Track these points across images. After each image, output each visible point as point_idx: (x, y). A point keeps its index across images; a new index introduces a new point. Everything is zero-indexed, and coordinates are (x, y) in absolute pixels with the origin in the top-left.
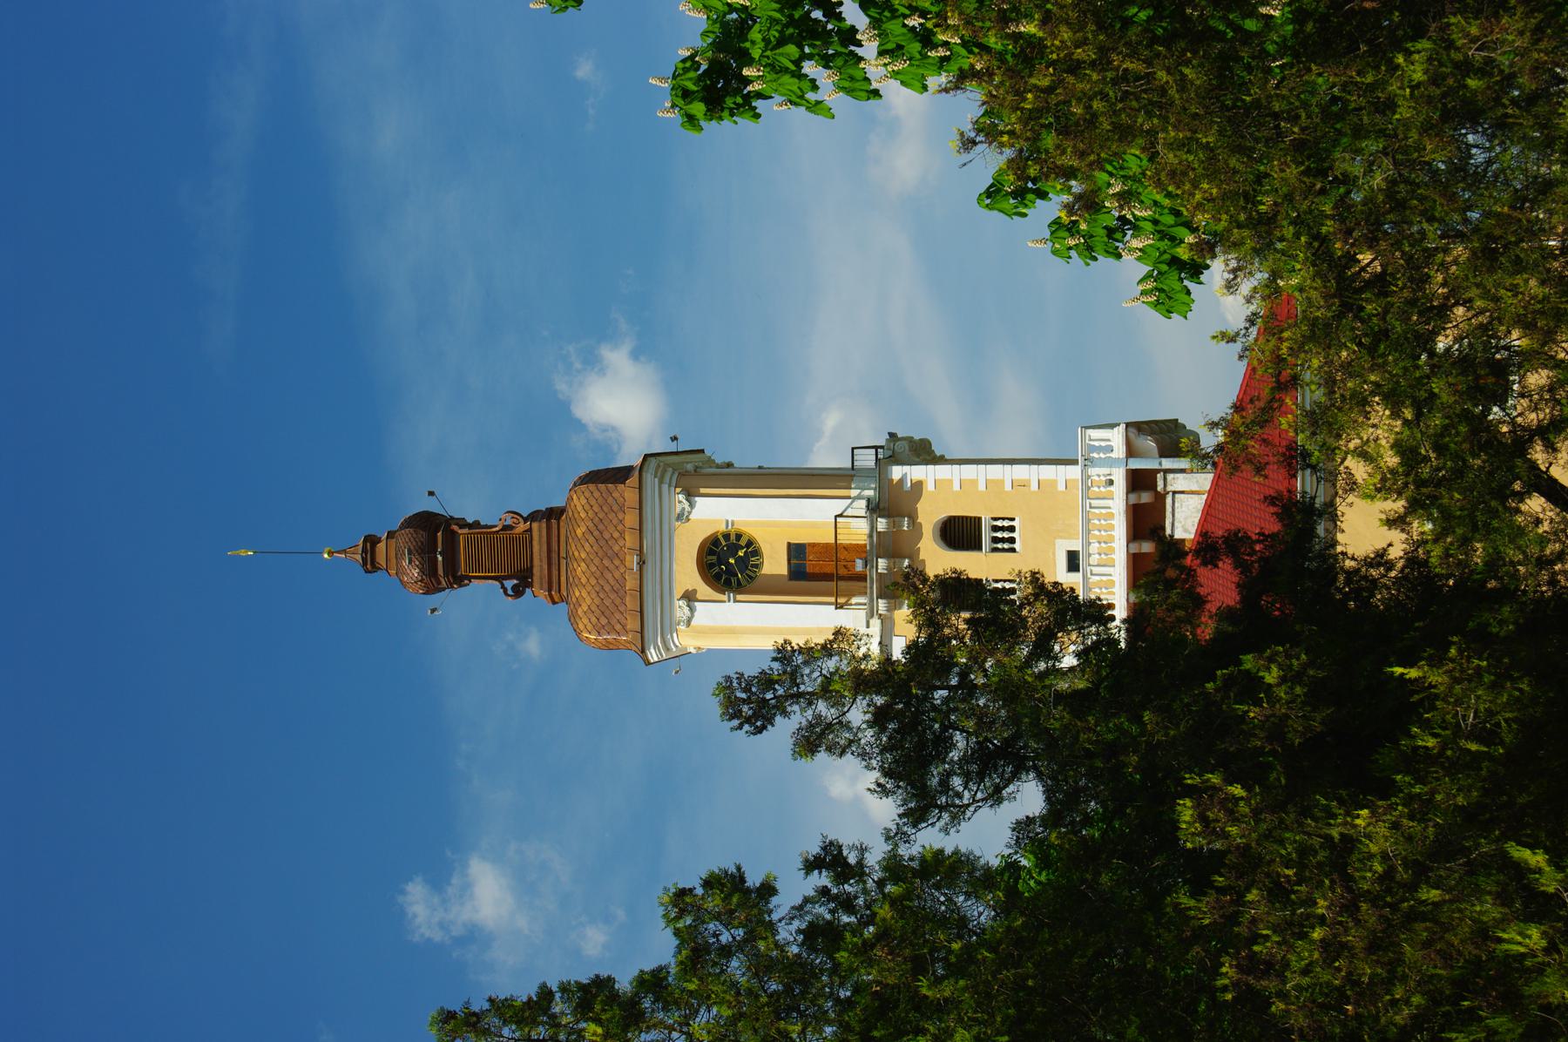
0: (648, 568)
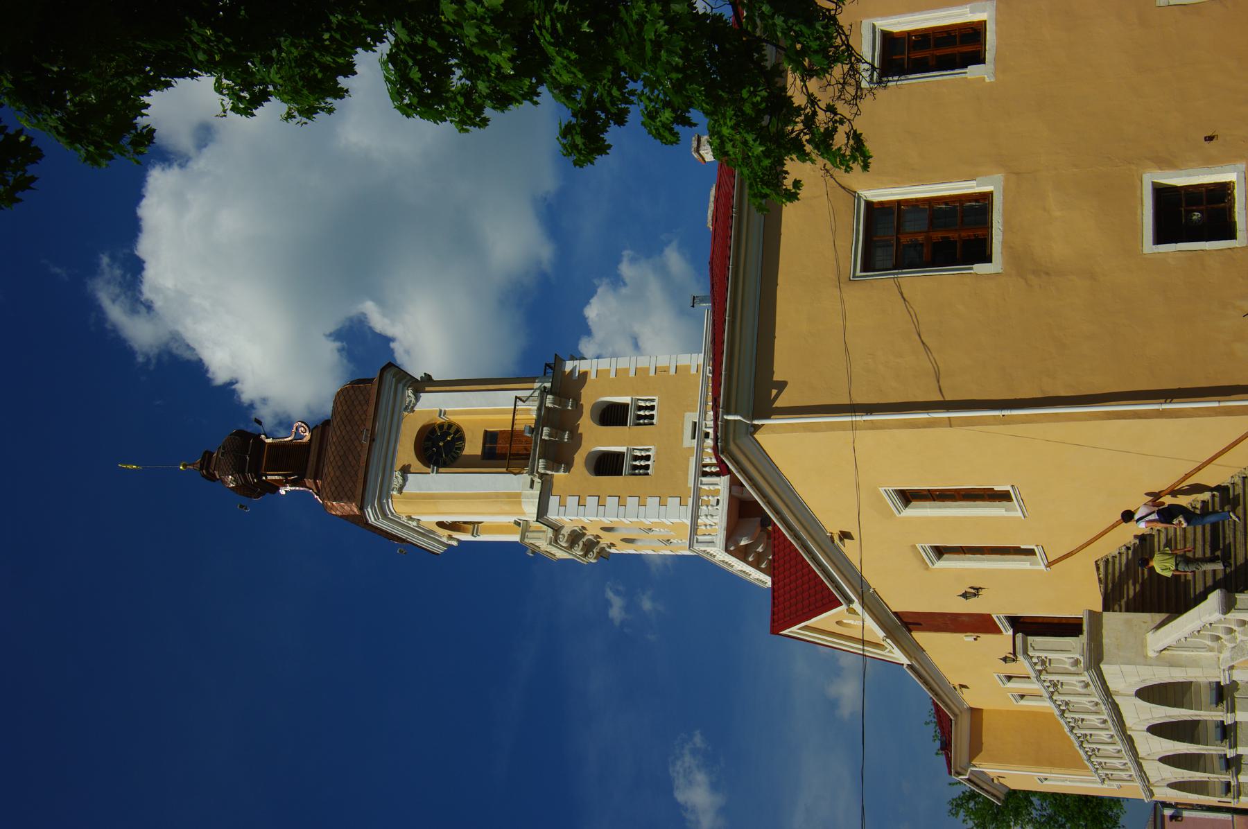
0: (377, 445)
